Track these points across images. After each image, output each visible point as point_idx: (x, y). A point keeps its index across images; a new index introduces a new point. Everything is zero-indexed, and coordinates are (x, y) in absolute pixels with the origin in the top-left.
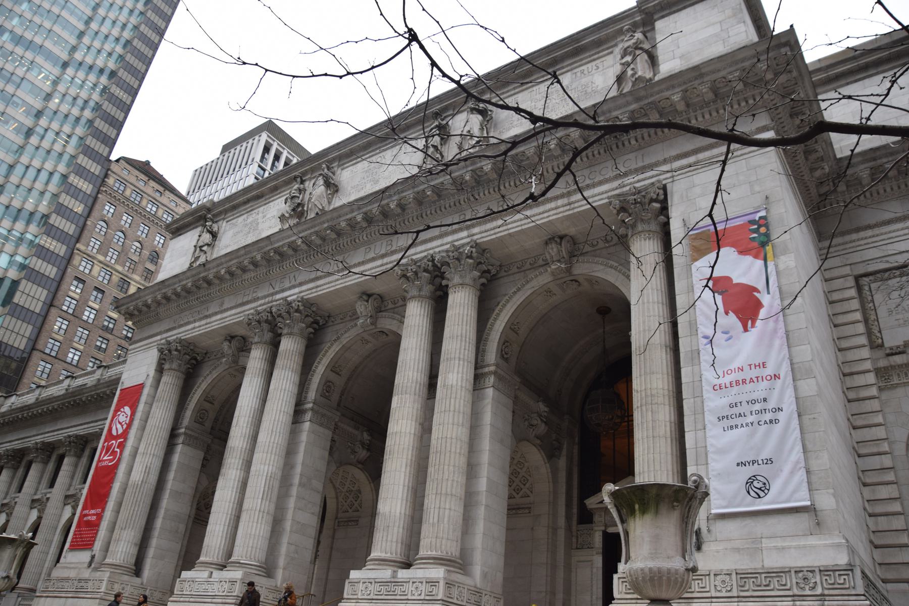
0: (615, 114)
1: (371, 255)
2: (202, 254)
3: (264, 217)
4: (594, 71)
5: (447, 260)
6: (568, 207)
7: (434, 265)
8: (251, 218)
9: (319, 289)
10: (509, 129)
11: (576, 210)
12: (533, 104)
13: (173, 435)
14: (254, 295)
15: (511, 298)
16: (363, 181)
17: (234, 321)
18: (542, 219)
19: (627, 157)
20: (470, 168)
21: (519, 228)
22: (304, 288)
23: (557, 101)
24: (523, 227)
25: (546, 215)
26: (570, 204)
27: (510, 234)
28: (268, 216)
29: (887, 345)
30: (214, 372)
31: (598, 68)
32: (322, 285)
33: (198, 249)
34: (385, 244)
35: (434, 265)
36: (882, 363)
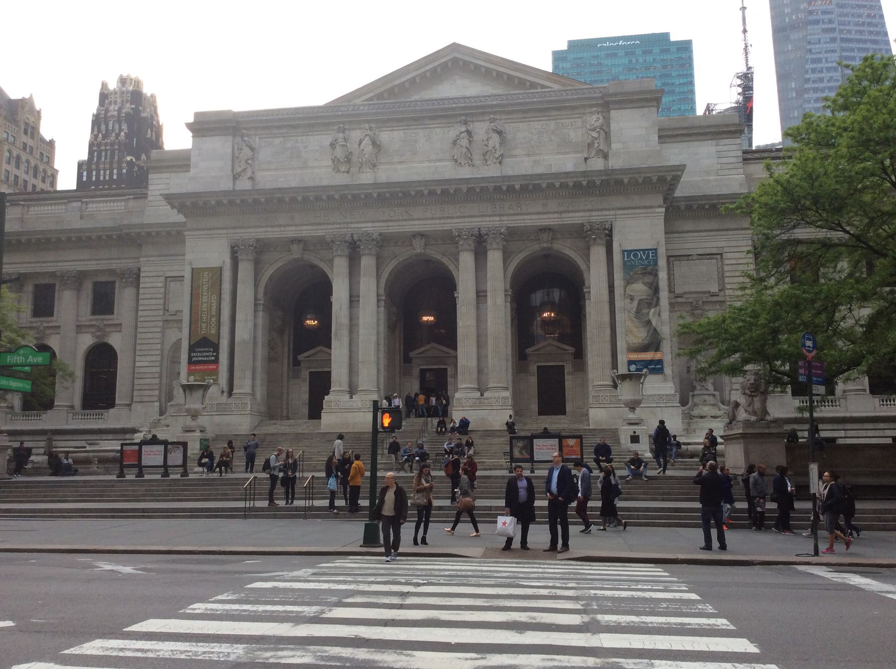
0: (594, 178)
3: (306, 147)
4: (569, 127)
5: (488, 232)
6: (560, 220)
7: (480, 234)
9: (389, 228)
12: (530, 135)
13: (255, 305)
20: (506, 183)
22: (377, 224)
29: (676, 292)
31: (572, 125)
33: (243, 163)
35: (480, 234)
36: (673, 301)
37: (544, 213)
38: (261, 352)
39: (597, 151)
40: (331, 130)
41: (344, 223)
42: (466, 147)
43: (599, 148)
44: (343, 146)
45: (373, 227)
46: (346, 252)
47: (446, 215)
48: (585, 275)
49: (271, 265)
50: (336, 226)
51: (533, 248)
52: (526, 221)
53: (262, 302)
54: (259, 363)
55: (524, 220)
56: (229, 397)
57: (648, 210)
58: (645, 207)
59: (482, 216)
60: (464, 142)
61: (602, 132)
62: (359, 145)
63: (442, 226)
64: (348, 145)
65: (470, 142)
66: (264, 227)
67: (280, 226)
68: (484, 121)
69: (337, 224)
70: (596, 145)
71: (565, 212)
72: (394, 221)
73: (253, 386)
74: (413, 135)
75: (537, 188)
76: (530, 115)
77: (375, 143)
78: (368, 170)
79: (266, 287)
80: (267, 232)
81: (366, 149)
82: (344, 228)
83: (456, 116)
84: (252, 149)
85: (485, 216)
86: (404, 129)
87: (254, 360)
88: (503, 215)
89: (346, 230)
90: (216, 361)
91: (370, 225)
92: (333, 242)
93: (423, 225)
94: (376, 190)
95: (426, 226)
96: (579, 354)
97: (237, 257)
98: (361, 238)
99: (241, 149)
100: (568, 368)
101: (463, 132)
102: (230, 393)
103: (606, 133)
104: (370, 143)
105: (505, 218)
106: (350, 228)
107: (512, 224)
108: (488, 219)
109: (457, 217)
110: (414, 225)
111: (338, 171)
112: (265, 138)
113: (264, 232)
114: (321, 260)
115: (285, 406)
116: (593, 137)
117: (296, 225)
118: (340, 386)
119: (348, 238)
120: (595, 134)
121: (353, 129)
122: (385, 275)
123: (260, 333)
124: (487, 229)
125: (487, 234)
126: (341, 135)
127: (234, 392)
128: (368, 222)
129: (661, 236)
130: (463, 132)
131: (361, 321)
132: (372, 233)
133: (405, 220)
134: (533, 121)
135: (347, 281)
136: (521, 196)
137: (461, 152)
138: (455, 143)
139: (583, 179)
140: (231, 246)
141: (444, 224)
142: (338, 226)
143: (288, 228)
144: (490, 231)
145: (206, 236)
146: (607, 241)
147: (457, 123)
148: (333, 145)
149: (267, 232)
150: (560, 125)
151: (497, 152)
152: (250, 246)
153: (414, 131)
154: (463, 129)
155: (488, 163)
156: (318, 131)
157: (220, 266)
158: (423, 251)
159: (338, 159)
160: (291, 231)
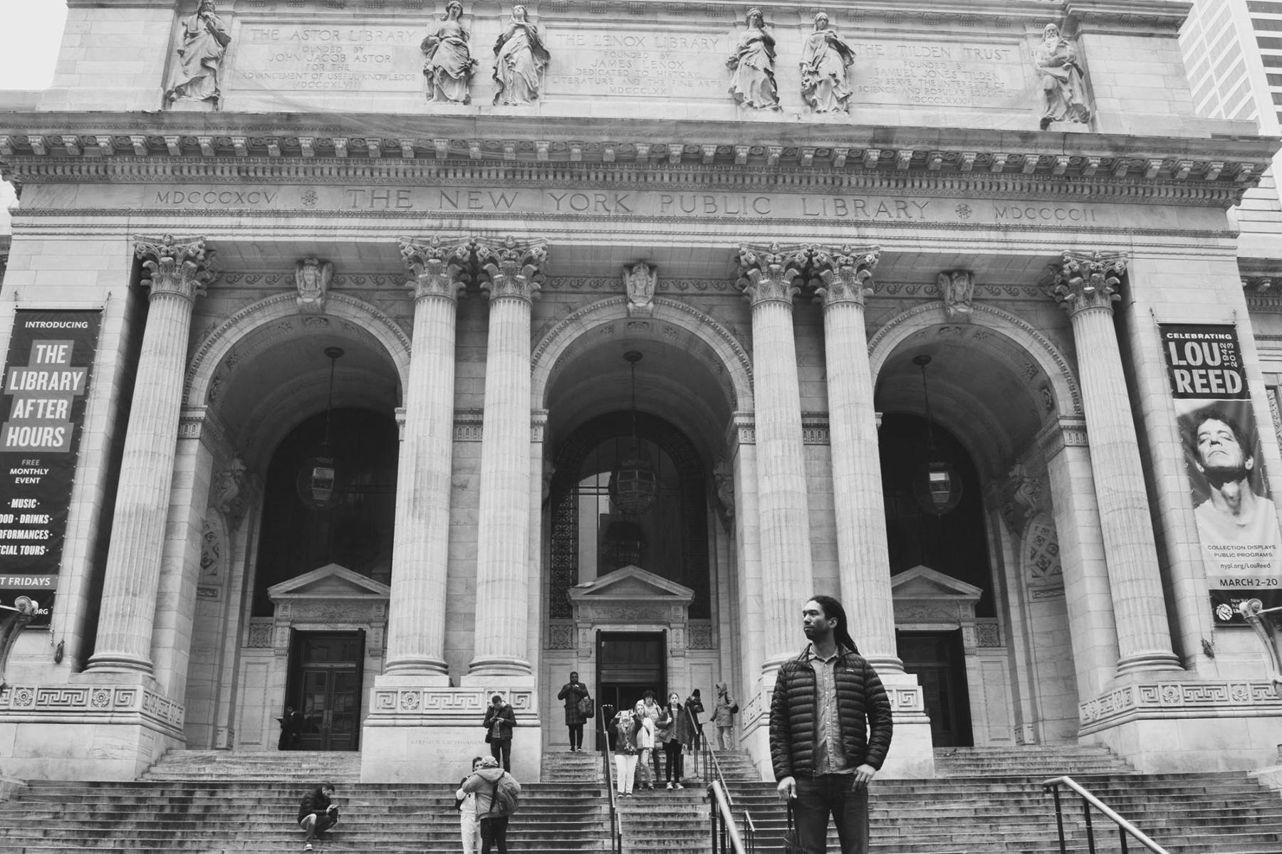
0: (1086, 153)
2: (208, 74)
4: (993, 60)
6: (1005, 245)
8: (319, 38)
9: (573, 236)
10: (875, 90)
11: (1014, 253)
13: (184, 421)
14: (403, 203)
15: (888, 331)
16: (602, 67)
17: (359, 240)
18: (968, 248)
19: (1073, 206)
21: (937, 251)
23: (947, 80)
24: (943, 251)
25: (974, 245)
26: (1006, 242)
27: (920, 254)
28: (367, 51)
30: (257, 314)
32: (577, 232)
34: (700, 200)
37: (964, 227)
38: (184, 550)
39: (1068, 107)
40: (427, 17)
42: (766, 70)
43: (1074, 102)
44: (457, 45)
45: (530, 231)
46: (453, 287)
47: (721, 214)
48: (1061, 390)
49: (236, 321)
50: (427, 222)
51: (925, 320)
52: (922, 243)
53: (202, 414)
54: (175, 583)
55: (918, 239)
56: (80, 671)
57: (1202, 241)
58: (1196, 234)
59: (814, 223)
60: (761, 60)
61: (1074, 70)
62: (497, 49)
63: (712, 238)
64: (469, 45)
65: (772, 62)
66: (232, 214)
67: (277, 214)
68: (799, 27)
69: (434, 216)
70: (1067, 95)
71: (1017, 228)
72: (586, 219)
73: (154, 645)
74: (629, 41)
75: (954, 166)
76: (906, 26)
77: (536, 47)
78: (518, 101)
79: (215, 379)
80: (240, 227)
81: (515, 56)
82: (451, 229)
83: (732, 11)
84: (222, 40)
85: (823, 223)
86: (607, 29)
87: (164, 572)
88: (866, 224)
89: (457, 233)
90: (50, 563)
91: (521, 224)
92: (417, 259)
93: (661, 233)
94: (546, 137)
95: (670, 237)
96: (986, 608)
97: (148, 288)
98: (496, 254)
99: (193, 35)
100: (970, 638)
101: (754, 40)
102: (84, 660)
103: (1081, 73)
104: (525, 42)
105: (870, 231)
107: (891, 248)
108: (827, 230)
109: (751, 222)
110: (638, 233)
111: (443, 97)
113: (231, 228)
114: (375, 316)
115: (224, 721)
116: (1056, 77)
117: (320, 214)
118: (421, 650)
119: (461, 250)
120: (1060, 72)
121: (481, 18)
122: (549, 361)
123: (186, 497)
124: (828, 253)
125: (828, 266)
126: (452, 25)
127: (96, 656)
128: (515, 217)
129: (1239, 301)
130: (754, 40)
131: (488, 468)
132: (528, 245)
133: (616, 219)
134: (912, 40)
135: (450, 361)
136: (909, 185)
137: (753, 82)
138: (733, 64)
139: (1060, 152)
140: (135, 255)
141: (715, 234)
142: (436, 223)
144: (835, 259)
145: (71, 230)
146: (1115, 304)
147: (735, 25)
148: (429, 47)
150: (973, 53)
151: (840, 86)
152: (188, 258)
153: (630, 34)
154: (757, 34)
155: (820, 107)
156: (393, 16)
157: (97, 307)
158: (651, 305)
159: (444, 71)
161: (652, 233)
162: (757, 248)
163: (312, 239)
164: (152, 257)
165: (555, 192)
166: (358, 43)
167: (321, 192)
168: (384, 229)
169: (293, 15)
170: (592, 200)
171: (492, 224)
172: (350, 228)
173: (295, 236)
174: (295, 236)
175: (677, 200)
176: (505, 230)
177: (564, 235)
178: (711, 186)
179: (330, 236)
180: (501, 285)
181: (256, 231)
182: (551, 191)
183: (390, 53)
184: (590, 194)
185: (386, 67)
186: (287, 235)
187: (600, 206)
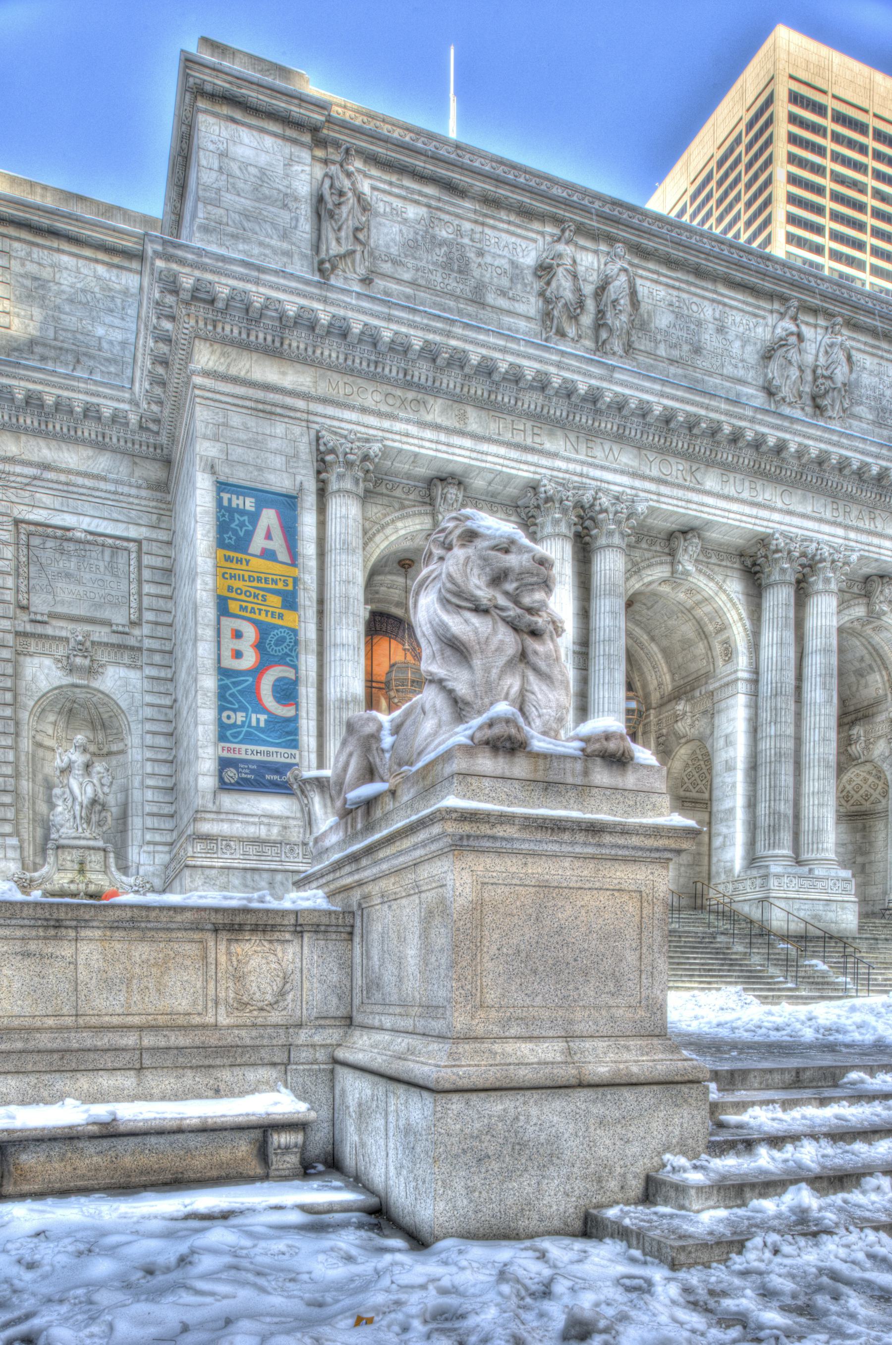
1: (730, 490)
3: (481, 253)
9: (663, 499)
14: (537, 440)
28: (488, 259)
34: (747, 484)
40: (538, 232)
41: (575, 461)
47: (760, 499)
80: (407, 435)
91: (625, 480)
95: (726, 514)
101: (792, 334)
106: (588, 477)
112: (384, 191)
117: (474, 436)
133: (688, 489)
141: (756, 518)
143: (457, 440)
149: (407, 435)
157: (294, 493)
160: (463, 448)
161: (716, 508)
162: (786, 537)
163: (466, 461)
164: (332, 451)
165: (648, 453)
166: (478, 245)
167: (472, 414)
168: (526, 463)
169: (420, 193)
170: (674, 468)
171: (598, 473)
172: (498, 456)
173: (453, 454)
174: (453, 454)
175: (732, 480)
176: (615, 484)
177: (655, 497)
178: (759, 474)
179: (482, 461)
180: (610, 533)
181: (420, 442)
182: (645, 452)
183: (507, 266)
184: (672, 460)
185: (505, 282)
186: (447, 453)
187: (680, 475)
